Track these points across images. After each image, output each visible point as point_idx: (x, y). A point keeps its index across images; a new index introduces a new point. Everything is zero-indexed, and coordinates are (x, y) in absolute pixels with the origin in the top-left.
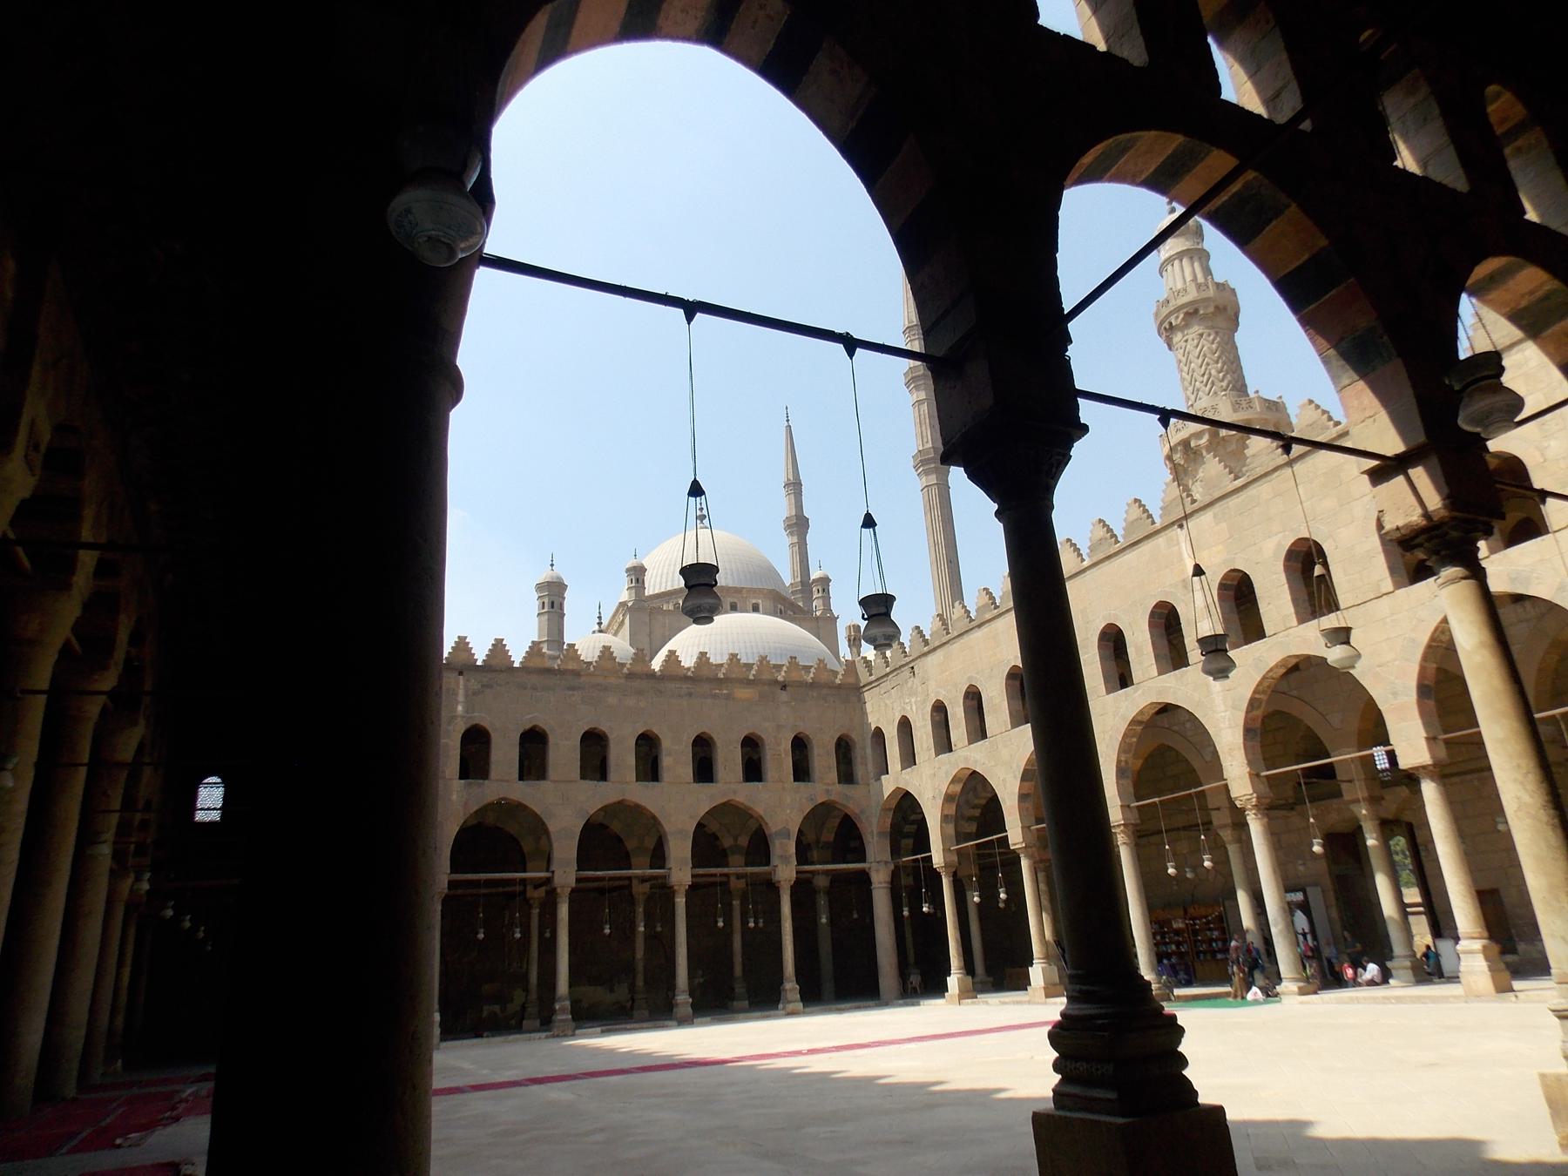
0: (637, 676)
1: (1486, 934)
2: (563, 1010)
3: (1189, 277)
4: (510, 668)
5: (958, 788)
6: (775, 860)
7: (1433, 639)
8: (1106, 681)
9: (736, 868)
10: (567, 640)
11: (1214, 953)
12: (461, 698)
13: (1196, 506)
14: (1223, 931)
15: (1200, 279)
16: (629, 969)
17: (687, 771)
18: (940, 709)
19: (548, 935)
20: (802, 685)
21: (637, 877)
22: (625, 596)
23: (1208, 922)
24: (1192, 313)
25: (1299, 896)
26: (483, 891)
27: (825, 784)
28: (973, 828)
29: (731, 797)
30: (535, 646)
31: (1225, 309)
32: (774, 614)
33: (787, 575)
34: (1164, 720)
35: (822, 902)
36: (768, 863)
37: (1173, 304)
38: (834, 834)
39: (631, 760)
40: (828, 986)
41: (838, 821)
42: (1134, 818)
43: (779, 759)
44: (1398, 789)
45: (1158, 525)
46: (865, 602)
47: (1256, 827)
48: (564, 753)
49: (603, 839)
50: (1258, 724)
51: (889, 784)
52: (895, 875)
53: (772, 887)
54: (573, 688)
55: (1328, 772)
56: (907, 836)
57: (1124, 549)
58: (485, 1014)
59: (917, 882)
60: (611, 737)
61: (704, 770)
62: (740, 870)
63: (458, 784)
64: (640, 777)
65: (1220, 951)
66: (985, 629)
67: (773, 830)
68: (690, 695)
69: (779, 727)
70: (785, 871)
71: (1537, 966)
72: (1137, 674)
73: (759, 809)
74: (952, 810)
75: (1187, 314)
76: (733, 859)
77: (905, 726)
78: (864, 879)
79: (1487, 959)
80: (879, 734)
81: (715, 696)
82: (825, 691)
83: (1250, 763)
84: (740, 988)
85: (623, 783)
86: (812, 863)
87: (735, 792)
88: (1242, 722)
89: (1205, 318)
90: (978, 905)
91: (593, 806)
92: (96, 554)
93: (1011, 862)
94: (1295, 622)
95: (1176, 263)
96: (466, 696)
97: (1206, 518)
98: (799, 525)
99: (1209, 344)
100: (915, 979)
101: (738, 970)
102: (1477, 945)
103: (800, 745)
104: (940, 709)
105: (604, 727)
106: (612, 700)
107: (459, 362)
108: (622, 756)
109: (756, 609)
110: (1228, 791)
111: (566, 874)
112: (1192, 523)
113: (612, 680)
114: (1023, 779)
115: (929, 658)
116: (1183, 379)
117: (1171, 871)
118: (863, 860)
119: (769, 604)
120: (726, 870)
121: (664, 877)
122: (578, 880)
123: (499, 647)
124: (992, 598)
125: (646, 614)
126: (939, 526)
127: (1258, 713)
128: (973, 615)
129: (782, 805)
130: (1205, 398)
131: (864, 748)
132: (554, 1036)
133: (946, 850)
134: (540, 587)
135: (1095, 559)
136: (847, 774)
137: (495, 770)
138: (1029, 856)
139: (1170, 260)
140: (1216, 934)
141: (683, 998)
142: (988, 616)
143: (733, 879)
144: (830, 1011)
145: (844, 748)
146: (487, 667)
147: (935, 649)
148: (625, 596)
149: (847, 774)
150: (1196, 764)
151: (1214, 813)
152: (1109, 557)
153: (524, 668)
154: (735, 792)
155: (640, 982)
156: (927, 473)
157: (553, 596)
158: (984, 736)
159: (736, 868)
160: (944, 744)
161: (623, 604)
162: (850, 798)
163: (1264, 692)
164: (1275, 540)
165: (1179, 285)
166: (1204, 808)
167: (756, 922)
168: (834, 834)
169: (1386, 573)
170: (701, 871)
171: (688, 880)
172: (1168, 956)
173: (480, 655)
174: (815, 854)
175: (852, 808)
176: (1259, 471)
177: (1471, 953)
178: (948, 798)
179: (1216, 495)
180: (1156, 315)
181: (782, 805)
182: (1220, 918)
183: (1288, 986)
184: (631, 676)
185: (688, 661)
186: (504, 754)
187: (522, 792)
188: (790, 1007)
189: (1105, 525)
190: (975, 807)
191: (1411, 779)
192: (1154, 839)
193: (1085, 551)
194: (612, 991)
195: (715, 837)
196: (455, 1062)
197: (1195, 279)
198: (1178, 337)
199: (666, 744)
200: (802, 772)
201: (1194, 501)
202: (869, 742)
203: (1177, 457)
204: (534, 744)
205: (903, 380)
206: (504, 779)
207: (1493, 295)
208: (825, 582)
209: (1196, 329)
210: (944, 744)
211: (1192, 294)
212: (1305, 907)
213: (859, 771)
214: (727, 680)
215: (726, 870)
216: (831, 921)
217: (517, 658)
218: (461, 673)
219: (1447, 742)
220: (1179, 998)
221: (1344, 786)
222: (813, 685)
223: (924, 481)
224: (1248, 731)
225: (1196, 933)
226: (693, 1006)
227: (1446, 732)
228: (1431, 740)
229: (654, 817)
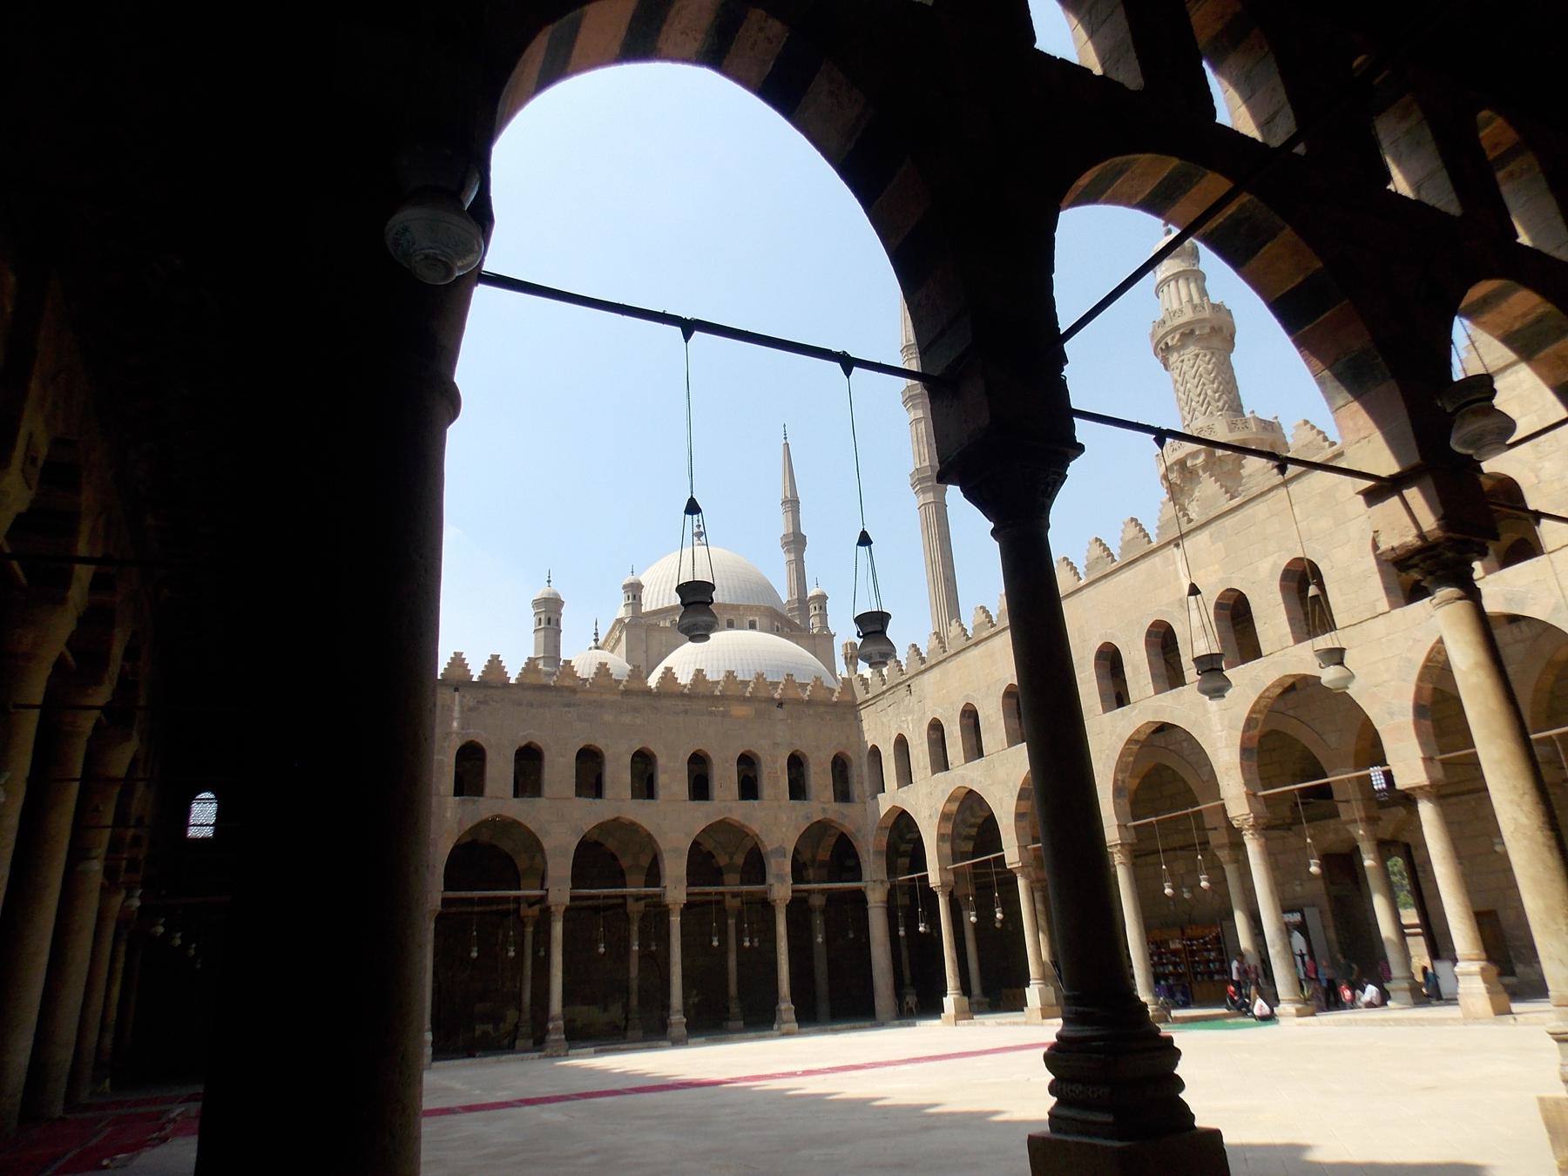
0: (633, 694)
1: (1484, 956)
2: (556, 1029)
3: (1185, 298)
4: (506, 685)
5: (954, 807)
6: (770, 879)
7: (1429, 659)
8: (1103, 701)
9: (732, 886)
10: (564, 656)
11: (1211, 974)
12: (456, 714)
13: (1192, 525)
14: (1220, 951)
15: (1196, 300)
16: (626, 990)
17: (683, 788)
18: (936, 728)
19: (542, 953)
21: (632, 895)
22: (622, 612)
23: (1205, 943)
24: (1188, 334)
25: (1296, 917)
26: (476, 909)
27: (822, 803)
28: (969, 846)
29: (727, 815)
30: (531, 663)
31: (1221, 329)
32: (771, 632)
33: (784, 593)
34: (1160, 740)
35: (818, 921)
36: (763, 881)
37: (1169, 325)
38: (831, 853)
39: (627, 777)
40: (824, 1007)
41: (834, 839)
42: (1131, 837)
43: (775, 777)
44: (1393, 810)
45: (1154, 544)
46: (861, 620)
47: (1253, 847)
48: (559, 770)
49: (599, 857)
50: (1255, 743)
51: (885, 803)
52: (891, 894)
53: (767, 906)
54: (568, 705)
55: (1325, 792)
56: (903, 855)
57: (1121, 568)
58: (478, 1033)
59: (913, 901)
60: (608, 755)
61: (700, 787)
62: (736, 889)
63: (452, 801)
64: (634, 796)
65: (1218, 972)
66: (982, 648)
68: (686, 712)
69: (776, 745)
70: (781, 890)
71: (1536, 989)
72: (1133, 693)
73: (755, 827)
74: (948, 829)
75: (1182, 334)
76: (728, 877)
77: (901, 744)
78: (859, 899)
79: (1485, 981)
80: (875, 752)
81: (711, 713)
82: (822, 709)
83: (1247, 782)
84: (735, 1008)
85: (619, 801)
86: (808, 882)
88: (1238, 742)
89: (1200, 339)
90: (974, 924)
91: (588, 824)
92: (93, 567)
93: (1008, 881)
94: (1291, 642)
95: (1172, 284)
96: (462, 712)
97: (1202, 537)
98: (796, 542)
99: (1205, 364)
100: (911, 1000)
101: (733, 988)
102: (1476, 967)
103: (796, 763)
104: (936, 728)
105: (600, 744)
106: (608, 717)
107: (456, 379)
108: (618, 774)
109: (752, 626)
110: (1225, 811)
111: (560, 892)
112: (1187, 543)
113: (608, 697)
114: (1020, 798)
115: (926, 676)
116: (1179, 399)
117: (1168, 891)
118: (859, 879)
119: (766, 621)
120: (721, 889)
121: (659, 896)
122: (573, 898)
123: (495, 663)
124: (989, 616)
125: (643, 632)
126: (936, 544)
127: (1255, 732)
128: (970, 633)
129: (778, 824)
130: (1201, 418)
131: (860, 766)
133: (942, 869)
134: (536, 603)
135: (1092, 578)
136: (843, 793)
137: (490, 787)
138: (1027, 876)
139: (1165, 281)
140: (1213, 954)
141: (677, 1018)
142: (985, 635)
143: (728, 898)
144: (825, 1032)
145: (840, 767)
146: (483, 683)
147: (932, 667)
148: (622, 612)
149: (843, 793)
150: (1193, 783)
151: (1210, 833)
152: (1105, 576)
153: (520, 684)
154: (730, 811)
155: (634, 1001)
156: (924, 491)
157: (550, 612)
158: (980, 754)
159: (732, 886)
160: (940, 762)
161: (619, 621)
162: (846, 817)
163: (1260, 712)
164: (1271, 560)
165: (1176, 306)
166: (1202, 828)
167: (751, 941)
168: (831, 853)
169: (1382, 593)
171: (683, 899)
172: (1166, 977)
173: (476, 671)
174: (811, 873)
175: (849, 827)
176: (1255, 491)
177: (1469, 975)
178: (945, 817)
179: (1212, 515)
180: (1153, 336)
181: (778, 824)
182: (1218, 939)
183: (1286, 1008)
184: (627, 693)
185: (684, 678)
186: (500, 770)
187: (517, 809)
188: (785, 1027)
189: (1101, 544)
190: (972, 826)
191: (1407, 800)
192: (1151, 859)
193: (1081, 570)
194: (605, 1010)
195: (710, 855)
196: (445, 1082)
197: (1191, 300)
198: (1175, 355)
199: (661, 761)
200: (798, 790)
201: (1190, 521)
202: (865, 760)
203: (1173, 476)
204: (529, 761)
205: (900, 399)
206: (501, 796)
207: (1487, 318)
208: (822, 599)
209: (1192, 350)
210: (940, 762)
211: (1188, 315)
212: (1302, 928)
213: (856, 790)
214: (723, 697)
215: (721, 889)
216: (827, 940)
217: (513, 673)
218: (456, 690)
219: (1443, 762)
220: (1176, 1020)
221: (1341, 807)
222: (810, 703)
223: (922, 499)
224: (1245, 751)
225: (1193, 953)
226: (687, 1025)
227: (1442, 752)
228: (1428, 760)
229: (649, 836)
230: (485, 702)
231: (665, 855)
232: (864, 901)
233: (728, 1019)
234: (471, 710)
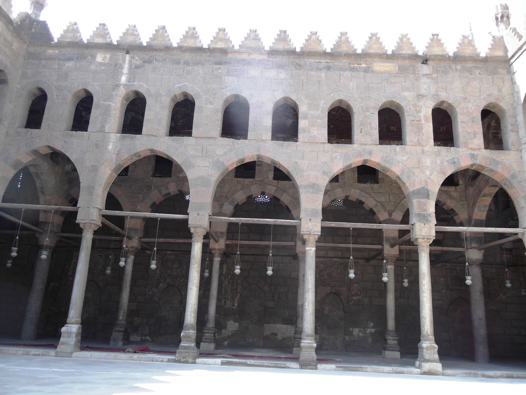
2: (188, 337)
12: (125, 70)
17: (324, 133)
19: (207, 274)
20: (444, 58)
39: (268, 122)
54: (220, 63)
60: (252, 102)
67: (411, 189)
68: (329, 68)
69: (420, 96)
82: (469, 65)
87: (370, 153)
96: (130, 69)
105: (245, 94)
131: (515, 116)
132: (175, 361)
154: (370, 153)
170: (333, 224)
199: (302, 109)
202: (520, 109)
214: (365, 55)
218: (128, 53)
226: (318, 350)
230: (149, 62)
231: (301, 191)
233: (385, 349)
234: (137, 67)
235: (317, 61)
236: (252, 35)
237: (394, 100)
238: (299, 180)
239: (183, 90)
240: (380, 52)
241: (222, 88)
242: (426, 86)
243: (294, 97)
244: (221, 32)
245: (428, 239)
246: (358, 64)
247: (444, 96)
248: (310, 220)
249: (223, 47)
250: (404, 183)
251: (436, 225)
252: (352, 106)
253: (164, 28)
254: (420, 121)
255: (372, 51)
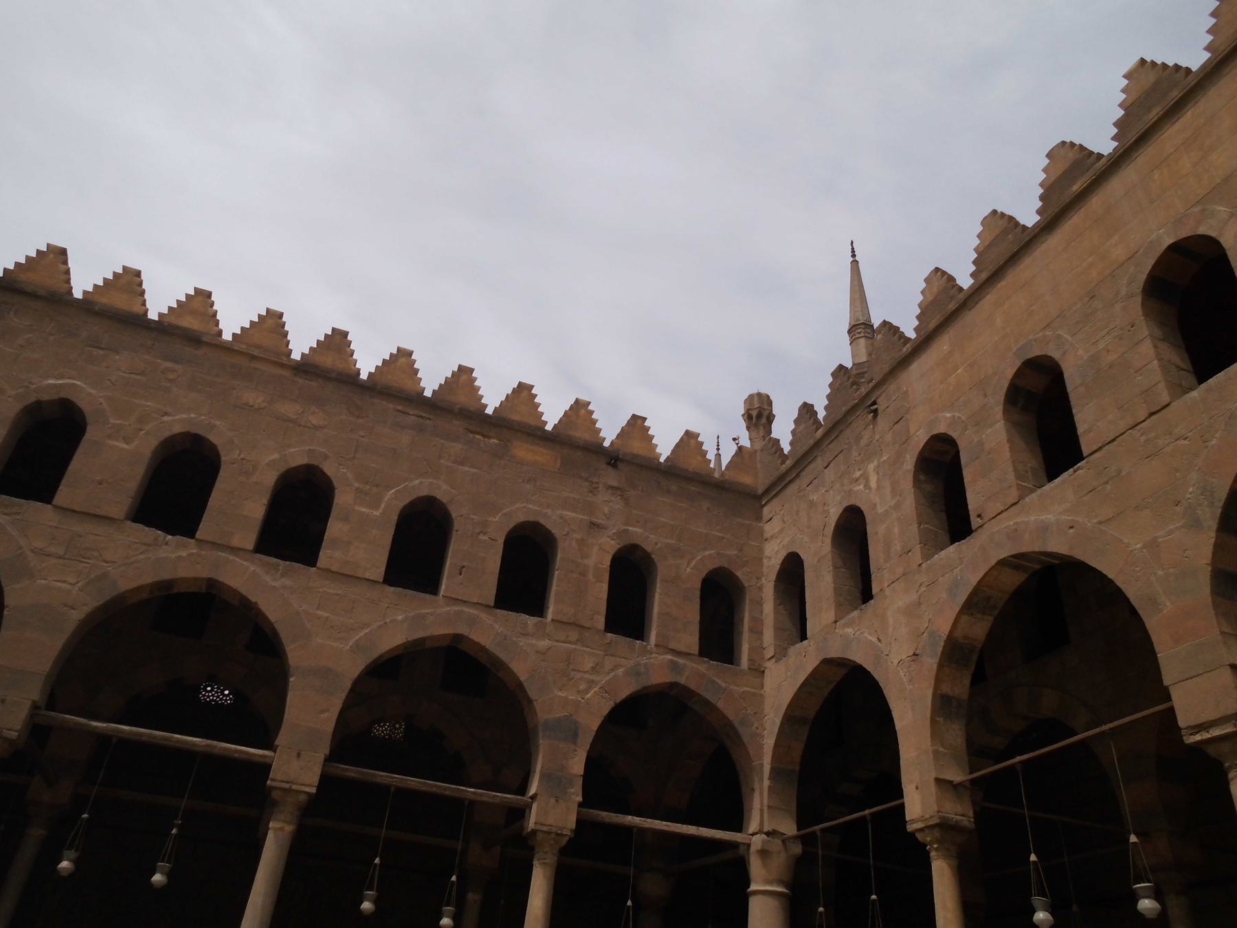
5: (979, 629)
39: (256, 509)
73: (521, 669)
85: (224, 550)
106: (255, 398)
118: (732, 814)
129: (571, 674)
136: (719, 639)
142: (1076, 187)
170: (352, 772)
181: (571, 674)
199: (342, 498)
232: (743, 877)
235: (400, 408)
236: (270, 322)
237: (542, 521)
238: (295, 654)
239: (63, 395)
240: (532, 421)
241: (166, 414)
242: (607, 504)
243: (329, 469)
244: (200, 298)
245: (558, 834)
246: (484, 436)
247: (639, 534)
248: (299, 755)
249: (195, 327)
250: (530, 701)
251: (580, 805)
252: (454, 515)
253: (63, 252)
254: (583, 574)
255: (516, 417)
